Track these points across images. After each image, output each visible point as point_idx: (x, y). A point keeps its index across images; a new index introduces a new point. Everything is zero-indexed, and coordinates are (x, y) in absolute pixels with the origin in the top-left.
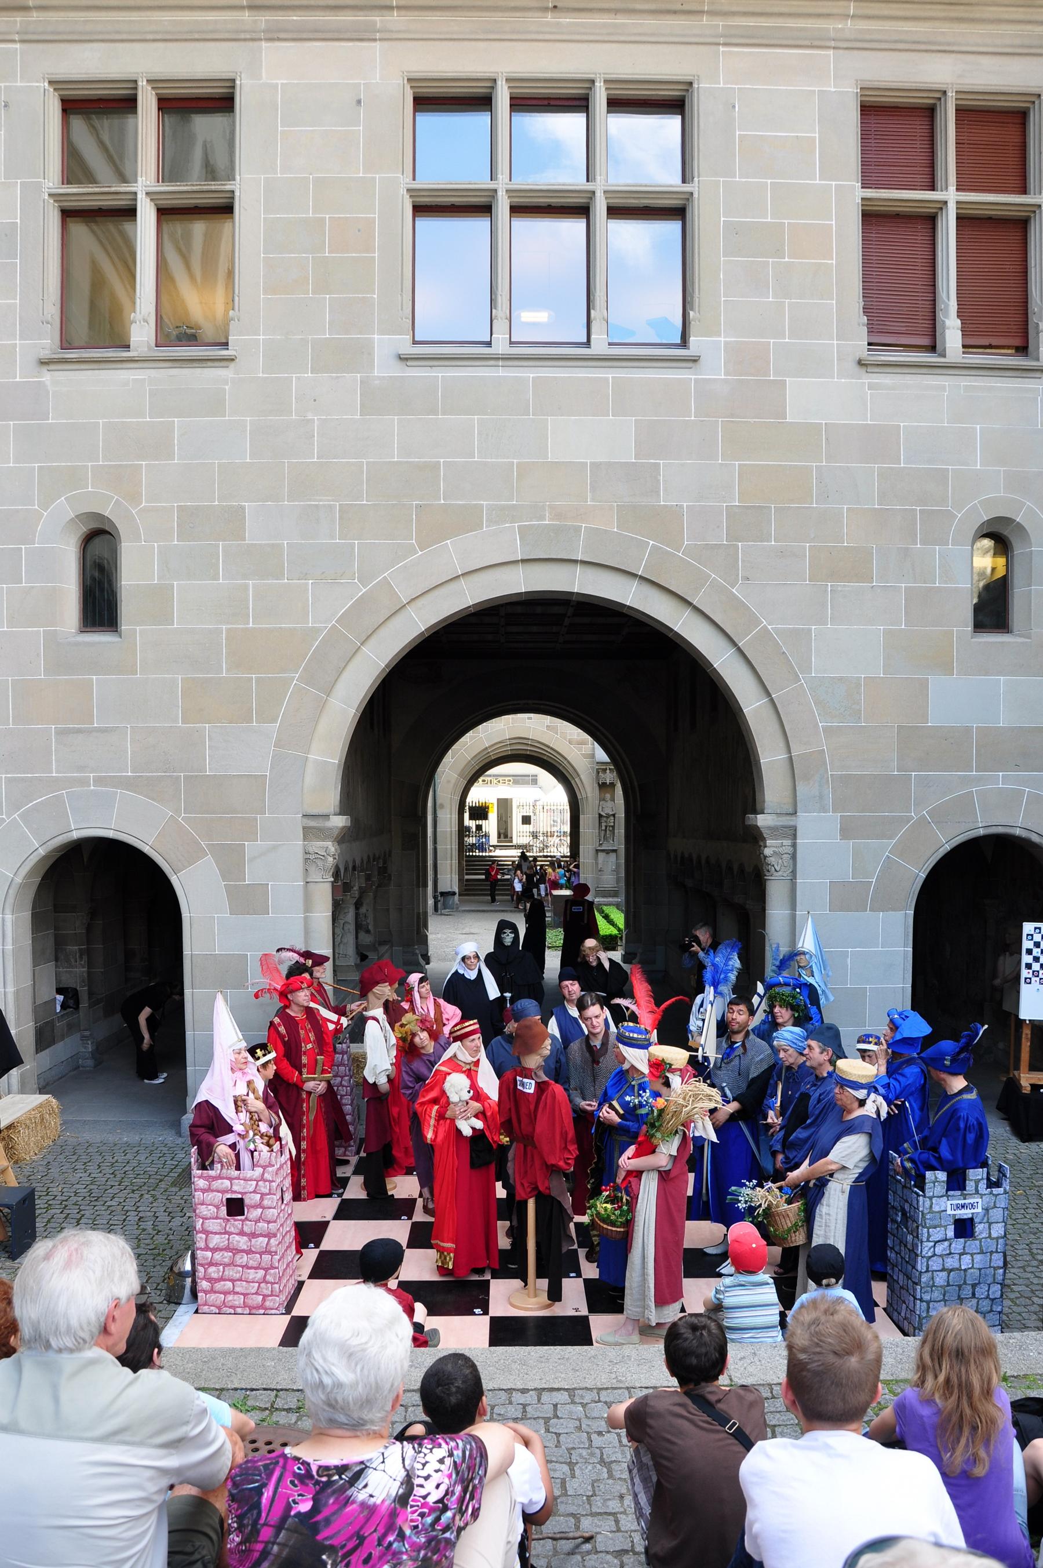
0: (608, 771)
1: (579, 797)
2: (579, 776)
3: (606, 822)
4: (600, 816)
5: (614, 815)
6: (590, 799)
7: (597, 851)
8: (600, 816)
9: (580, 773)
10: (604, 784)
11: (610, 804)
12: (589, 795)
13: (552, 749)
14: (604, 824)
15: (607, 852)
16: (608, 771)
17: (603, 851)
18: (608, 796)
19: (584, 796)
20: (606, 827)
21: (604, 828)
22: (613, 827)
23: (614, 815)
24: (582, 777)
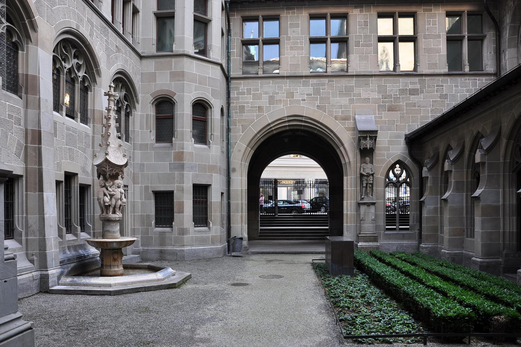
0: (368, 138)
1: (343, 162)
2: (343, 145)
3: (367, 180)
4: (362, 175)
5: (372, 175)
6: (352, 163)
7: (359, 205)
8: (362, 175)
9: (344, 143)
10: (365, 149)
11: (369, 165)
12: (351, 160)
13: (321, 124)
14: (365, 182)
15: (369, 205)
16: (368, 138)
17: (364, 204)
18: (368, 159)
19: (347, 161)
20: (367, 184)
21: (365, 185)
22: (372, 184)
23: (372, 175)
24: (346, 145)
